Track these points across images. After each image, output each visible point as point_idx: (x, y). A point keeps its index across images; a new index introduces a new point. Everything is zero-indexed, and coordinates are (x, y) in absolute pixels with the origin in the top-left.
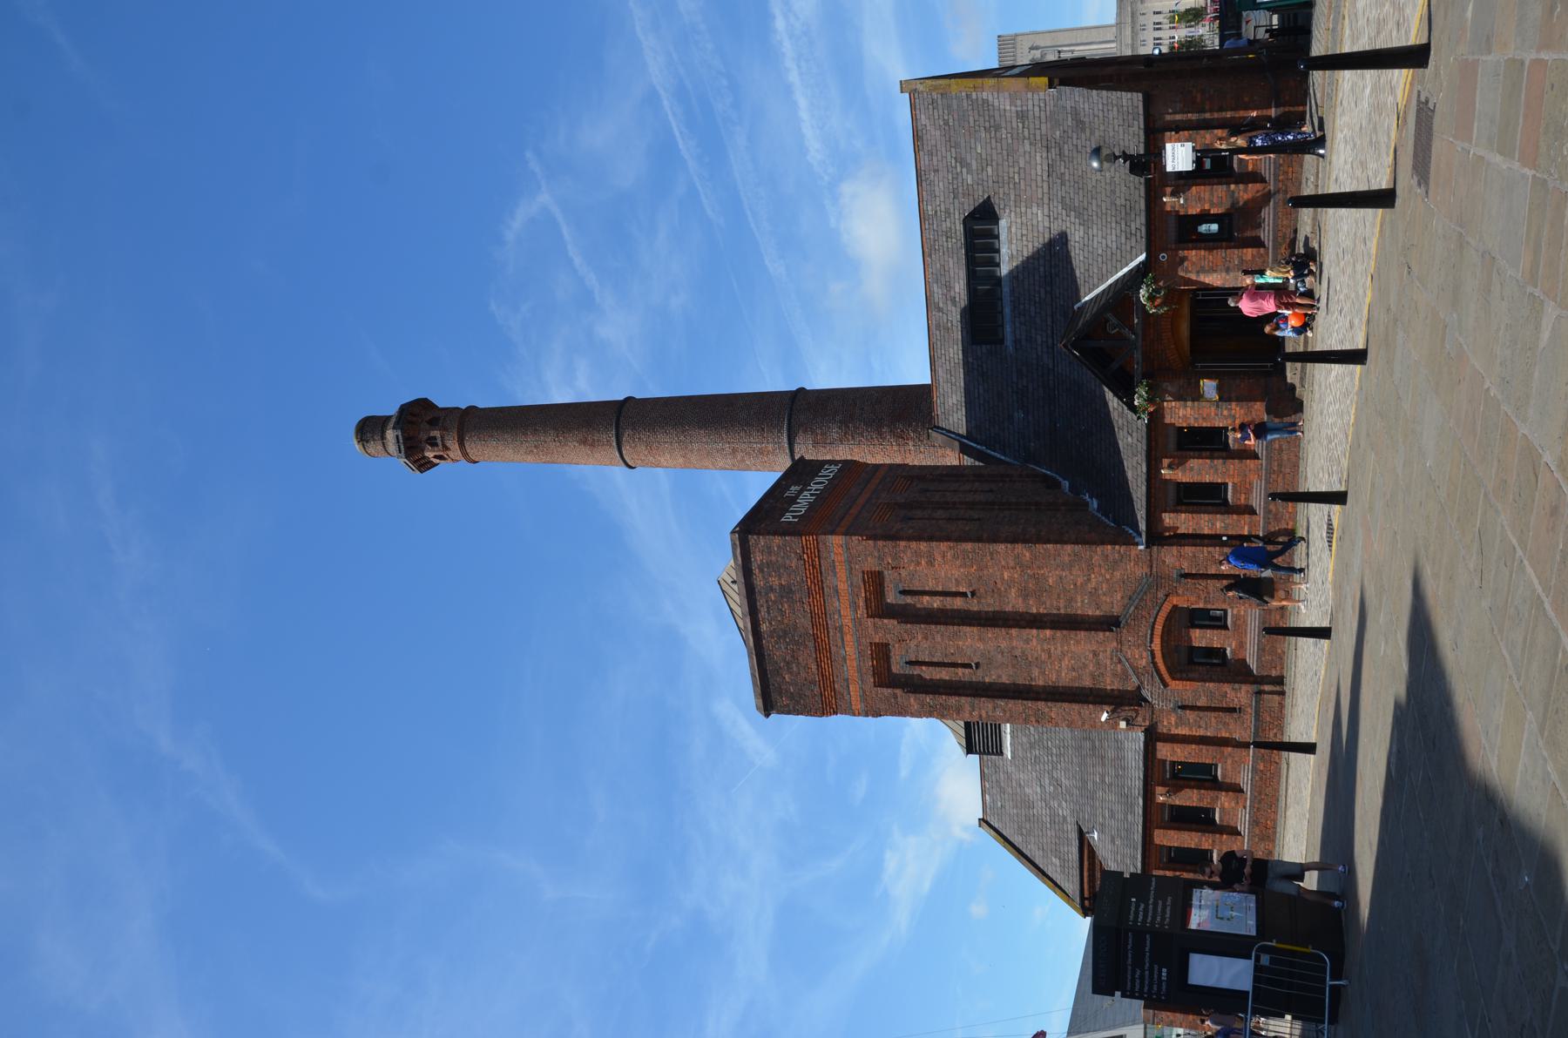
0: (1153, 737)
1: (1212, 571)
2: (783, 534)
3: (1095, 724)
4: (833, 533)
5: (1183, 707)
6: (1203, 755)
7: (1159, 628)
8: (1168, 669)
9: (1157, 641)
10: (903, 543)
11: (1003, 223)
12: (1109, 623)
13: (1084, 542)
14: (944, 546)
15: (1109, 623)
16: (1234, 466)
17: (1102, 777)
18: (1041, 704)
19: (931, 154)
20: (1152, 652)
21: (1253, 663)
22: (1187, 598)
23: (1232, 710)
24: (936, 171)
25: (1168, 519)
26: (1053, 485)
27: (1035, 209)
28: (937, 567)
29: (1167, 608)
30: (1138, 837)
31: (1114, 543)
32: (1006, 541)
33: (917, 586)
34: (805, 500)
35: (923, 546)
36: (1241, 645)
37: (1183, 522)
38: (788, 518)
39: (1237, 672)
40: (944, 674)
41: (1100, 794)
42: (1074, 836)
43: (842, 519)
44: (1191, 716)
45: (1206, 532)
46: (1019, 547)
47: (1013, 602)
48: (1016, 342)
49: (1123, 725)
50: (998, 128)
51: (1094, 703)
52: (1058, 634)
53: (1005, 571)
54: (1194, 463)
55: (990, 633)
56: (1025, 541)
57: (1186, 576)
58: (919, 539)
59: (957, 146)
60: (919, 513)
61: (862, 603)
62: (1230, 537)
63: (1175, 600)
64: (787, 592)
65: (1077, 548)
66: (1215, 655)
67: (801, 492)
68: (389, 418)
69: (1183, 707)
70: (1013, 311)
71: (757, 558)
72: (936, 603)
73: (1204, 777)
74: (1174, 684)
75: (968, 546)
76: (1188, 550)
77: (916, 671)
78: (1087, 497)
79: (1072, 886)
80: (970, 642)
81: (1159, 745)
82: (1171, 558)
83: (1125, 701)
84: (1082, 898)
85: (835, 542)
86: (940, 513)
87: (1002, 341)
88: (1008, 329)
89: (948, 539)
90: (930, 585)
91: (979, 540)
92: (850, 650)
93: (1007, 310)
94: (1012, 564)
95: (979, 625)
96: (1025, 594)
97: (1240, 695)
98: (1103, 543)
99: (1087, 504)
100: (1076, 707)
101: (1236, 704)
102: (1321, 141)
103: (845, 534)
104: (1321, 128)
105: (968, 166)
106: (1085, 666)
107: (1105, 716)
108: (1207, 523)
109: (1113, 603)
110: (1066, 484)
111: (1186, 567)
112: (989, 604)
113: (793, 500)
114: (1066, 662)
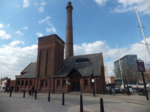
0: (35, 78)
3: (36, 72)
7: (45, 79)
9: (44, 79)
12: (46, 74)
13: (54, 71)
15: (46, 74)
18: (38, 67)
21: (42, 89)
22: (48, 82)
25: (56, 79)
28: (52, 56)
29: (47, 80)
30: (25, 77)
32: (54, 62)
34: (60, 42)
36: (44, 88)
37: (56, 81)
38: (58, 40)
39: (41, 88)
44: (37, 83)
46: (54, 64)
47: (48, 63)
53: (52, 62)
64: (50, 40)
65: (54, 70)
66: (43, 85)
71: (53, 37)
72: (49, 55)
74: (40, 81)
76: (53, 82)
77: (42, 54)
80: (45, 59)
82: (52, 80)
83: (38, 75)
85: (55, 45)
90: (50, 55)
92: (44, 47)
97: (39, 88)
102: (95, 96)
103: (56, 46)
104: (96, 96)
108: (56, 84)
109: (48, 74)
112: (48, 61)
113: (60, 41)
114: (42, 69)
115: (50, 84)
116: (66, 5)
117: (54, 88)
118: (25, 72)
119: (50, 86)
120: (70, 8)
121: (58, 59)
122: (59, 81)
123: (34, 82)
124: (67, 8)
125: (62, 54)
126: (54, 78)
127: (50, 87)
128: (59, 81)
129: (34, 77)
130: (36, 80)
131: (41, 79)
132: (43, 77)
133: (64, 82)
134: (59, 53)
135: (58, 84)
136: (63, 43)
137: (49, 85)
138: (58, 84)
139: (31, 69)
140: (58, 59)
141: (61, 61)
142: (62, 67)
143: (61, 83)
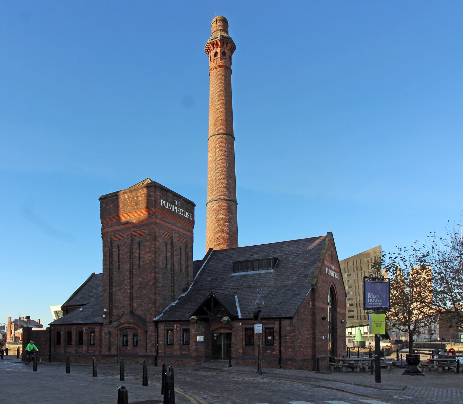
1: (148, 341)
5: (110, 334)
11: (272, 271)
17: (96, 311)
18: (108, 291)
19: (304, 244)
20: (124, 324)
24: (297, 247)
26: (184, 291)
27: (273, 281)
29: (137, 327)
30: (74, 322)
33: (142, 248)
38: (163, 202)
40: (116, 259)
41: (92, 310)
42: (84, 303)
43: (164, 221)
45: (159, 339)
48: (233, 277)
50: (305, 268)
60: (169, 247)
62: (158, 346)
67: (177, 206)
68: (228, 33)
69: (110, 334)
70: (243, 275)
79: (70, 304)
81: (99, 327)
82: (151, 328)
84: (66, 306)
86: (169, 254)
87: (234, 272)
88: (237, 274)
90: (142, 253)
93: (243, 273)
94: (148, 279)
96: (140, 283)
99: (174, 302)
100: (108, 302)
101: (112, 350)
104: (265, 373)
105: (296, 258)
106: (120, 303)
107: (105, 310)
110: (184, 295)
111: (149, 333)
113: (172, 203)
114: (121, 297)
119: (147, 345)
121: (169, 265)
123: (101, 335)
125: (186, 244)
130: (105, 330)
134: (172, 244)
139: (91, 296)
140: (169, 265)
141: (183, 269)
142: (187, 288)
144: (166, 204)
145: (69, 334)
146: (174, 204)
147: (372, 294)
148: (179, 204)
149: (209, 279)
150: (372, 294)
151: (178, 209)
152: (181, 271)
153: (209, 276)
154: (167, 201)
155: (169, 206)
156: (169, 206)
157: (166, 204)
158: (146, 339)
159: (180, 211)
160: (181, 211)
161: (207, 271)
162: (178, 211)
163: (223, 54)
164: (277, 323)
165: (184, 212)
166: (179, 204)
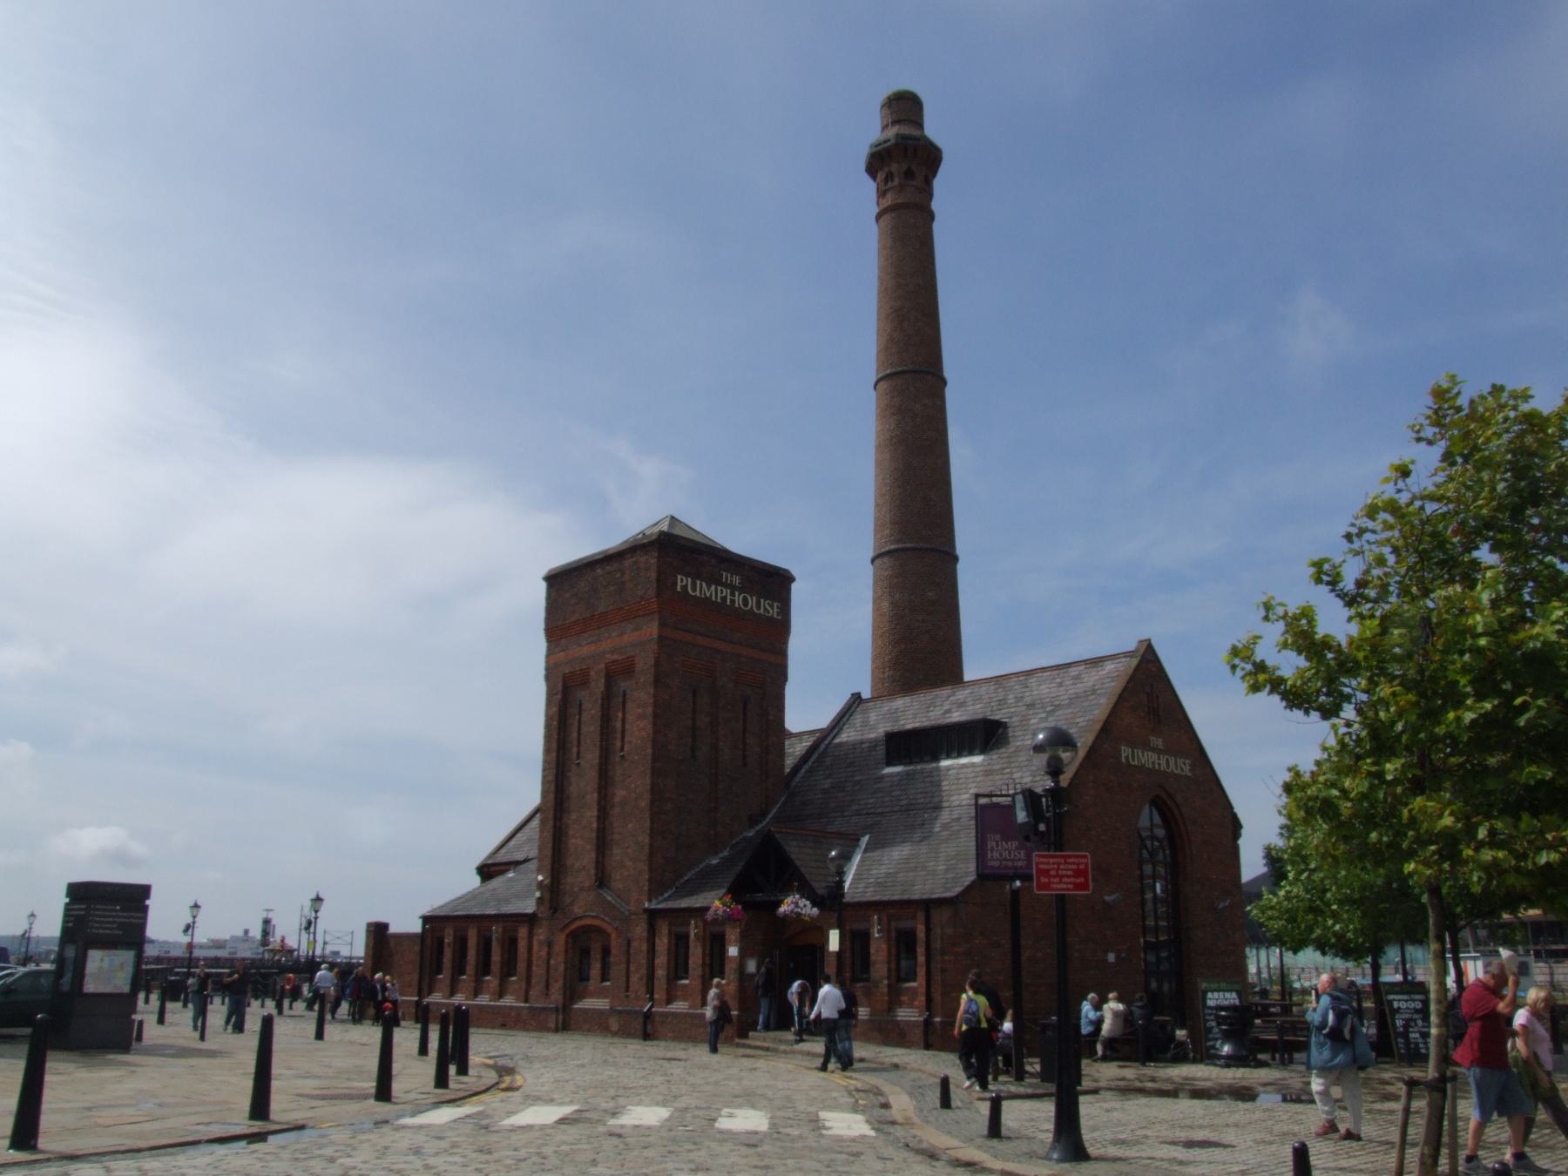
0: (530, 920)
1: (632, 968)
2: (658, 580)
4: (662, 625)
6: (521, 966)
7: (597, 922)
8: (572, 932)
10: (652, 691)
13: (651, 854)
14: (650, 728)
16: (697, 983)
19: (1078, 677)
23: (547, 987)
29: (609, 929)
30: (476, 911)
31: (650, 881)
33: (629, 705)
34: (714, 593)
35: (650, 710)
37: (662, 943)
38: (682, 581)
44: (544, 953)
46: (647, 796)
49: (538, 894)
51: (553, 869)
52: (594, 835)
54: (699, 951)
55: (594, 774)
56: (652, 803)
57: (629, 944)
58: (656, 705)
59: (1068, 706)
61: (615, 657)
63: (614, 935)
71: (642, 559)
73: (509, 968)
75: (649, 751)
76: (645, 947)
78: (726, 853)
82: (640, 930)
83: (553, 893)
89: (656, 732)
90: (630, 718)
91: (655, 759)
92: (586, 650)
95: (601, 764)
97: (556, 996)
98: (651, 870)
99: (716, 853)
103: (660, 636)
108: (661, 960)
111: (635, 944)
115: (628, 962)
116: (871, 130)
117: (652, 999)
118: (505, 859)
119: (628, 977)
120: (905, 162)
122: (680, 943)
124: (872, 170)
126: (653, 915)
127: (627, 989)
128: (680, 943)
129: (529, 906)
130: (541, 934)
131: (574, 926)
132: (582, 906)
133: (717, 944)
135: (679, 968)
136: (773, 582)
137: (617, 970)
138: (679, 968)
142: (764, 814)
143: (696, 954)
144: (694, 585)
145: (461, 943)
146: (718, 582)
147: (998, 837)
148: (736, 580)
149: (827, 784)
150: (998, 837)
151: (733, 594)
152: (745, 765)
153: (828, 777)
154: (696, 576)
155: (703, 590)
156: (703, 590)
157: (694, 585)
158: (628, 962)
159: (739, 599)
160: (745, 600)
161: (828, 760)
162: (733, 601)
163: (909, 174)
164: (921, 915)
165: (752, 601)
166: (736, 580)
